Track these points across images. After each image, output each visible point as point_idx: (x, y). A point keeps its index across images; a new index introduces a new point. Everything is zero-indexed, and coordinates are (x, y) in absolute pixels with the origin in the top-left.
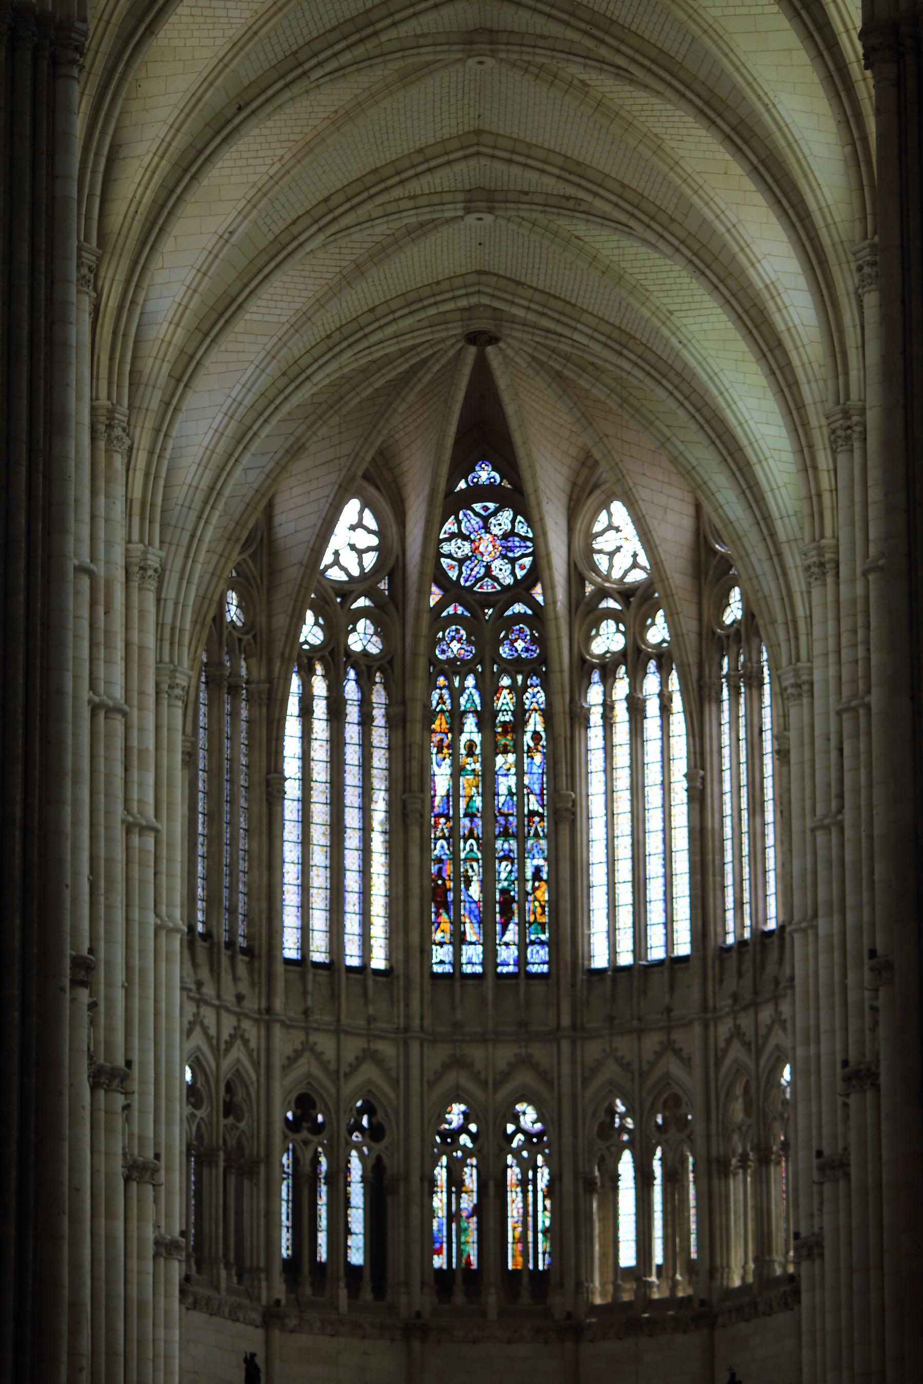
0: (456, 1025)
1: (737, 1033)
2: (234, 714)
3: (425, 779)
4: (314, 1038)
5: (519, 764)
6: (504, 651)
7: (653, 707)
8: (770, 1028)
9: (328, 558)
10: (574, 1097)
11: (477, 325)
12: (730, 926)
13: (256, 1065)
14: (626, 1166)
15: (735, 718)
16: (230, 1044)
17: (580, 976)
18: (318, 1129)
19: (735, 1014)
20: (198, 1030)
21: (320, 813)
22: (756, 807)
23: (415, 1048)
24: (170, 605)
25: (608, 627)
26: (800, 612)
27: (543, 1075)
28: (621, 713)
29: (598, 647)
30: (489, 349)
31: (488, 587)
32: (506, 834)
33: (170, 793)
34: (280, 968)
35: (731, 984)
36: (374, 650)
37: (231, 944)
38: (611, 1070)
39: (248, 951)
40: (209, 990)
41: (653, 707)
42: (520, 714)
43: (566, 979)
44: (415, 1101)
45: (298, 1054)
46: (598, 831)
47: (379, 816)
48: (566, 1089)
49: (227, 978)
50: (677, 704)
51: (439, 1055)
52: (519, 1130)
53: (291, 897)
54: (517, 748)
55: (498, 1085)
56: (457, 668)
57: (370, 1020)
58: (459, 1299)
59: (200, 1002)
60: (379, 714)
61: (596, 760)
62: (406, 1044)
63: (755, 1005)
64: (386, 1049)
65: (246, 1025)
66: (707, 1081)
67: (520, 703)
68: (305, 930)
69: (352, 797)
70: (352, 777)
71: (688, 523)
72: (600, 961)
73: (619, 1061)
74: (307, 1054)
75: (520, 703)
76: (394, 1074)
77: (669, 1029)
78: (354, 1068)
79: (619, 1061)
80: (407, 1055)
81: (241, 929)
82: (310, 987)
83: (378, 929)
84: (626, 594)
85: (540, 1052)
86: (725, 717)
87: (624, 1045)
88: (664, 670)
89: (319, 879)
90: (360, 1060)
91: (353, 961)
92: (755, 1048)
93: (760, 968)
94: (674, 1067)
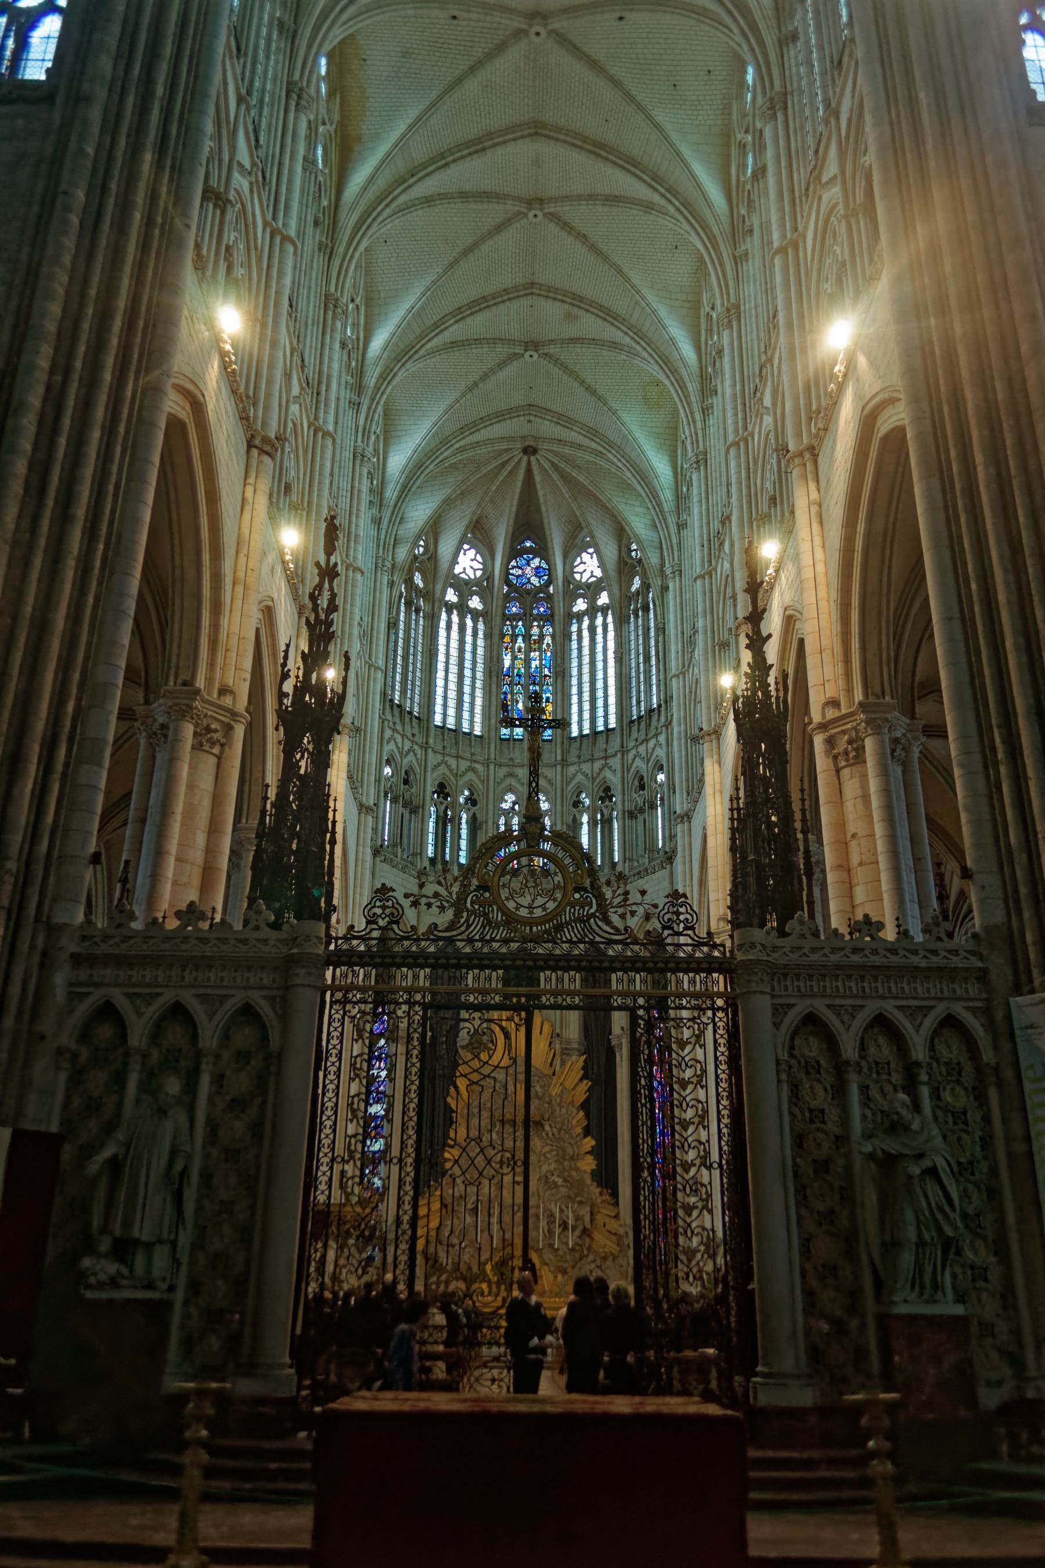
0: (511, 759)
2: (417, 621)
3: (500, 661)
4: (447, 758)
5: (540, 656)
6: (535, 612)
7: (600, 630)
11: (527, 444)
12: (635, 712)
13: (420, 766)
14: (585, 819)
15: (637, 627)
16: (408, 753)
19: (637, 746)
21: (454, 669)
22: (647, 659)
23: (492, 767)
24: (384, 532)
25: (580, 601)
26: (674, 541)
28: (586, 634)
29: (575, 609)
30: (533, 458)
31: (529, 586)
32: (534, 684)
33: (358, 504)
34: (432, 729)
35: (635, 735)
36: (480, 607)
37: (410, 713)
38: (580, 777)
40: (399, 727)
41: (600, 630)
42: (542, 637)
44: (491, 789)
45: (439, 764)
46: (574, 681)
47: (479, 675)
48: (559, 786)
49: (408, 727)
50: (611, 627)
51: (503, 771)
53: (439, 700)
54: (540, 650)
56: (515, 617)
57: (473, 754)
59: (394, 730)
60: (481, 634)
63: (647, 740)
64: (480, 767)
65: (416, 747)
67: (541, 632)
68: (445, 715)
69: (468, 664)
70: (468, 656)
71: (616, 552)
73: (583, 774)
74: (443, 766)
75: (541, 632)
77: (606, 758)
78: (464, 773)
79: (583, 774)
81: (416, 709)
83: (478, 718)
84: (588, 586)
86: (632, 628)
87: (586, 767)
88: (605, 616)
89: (452, 694)
90: (467, 771)
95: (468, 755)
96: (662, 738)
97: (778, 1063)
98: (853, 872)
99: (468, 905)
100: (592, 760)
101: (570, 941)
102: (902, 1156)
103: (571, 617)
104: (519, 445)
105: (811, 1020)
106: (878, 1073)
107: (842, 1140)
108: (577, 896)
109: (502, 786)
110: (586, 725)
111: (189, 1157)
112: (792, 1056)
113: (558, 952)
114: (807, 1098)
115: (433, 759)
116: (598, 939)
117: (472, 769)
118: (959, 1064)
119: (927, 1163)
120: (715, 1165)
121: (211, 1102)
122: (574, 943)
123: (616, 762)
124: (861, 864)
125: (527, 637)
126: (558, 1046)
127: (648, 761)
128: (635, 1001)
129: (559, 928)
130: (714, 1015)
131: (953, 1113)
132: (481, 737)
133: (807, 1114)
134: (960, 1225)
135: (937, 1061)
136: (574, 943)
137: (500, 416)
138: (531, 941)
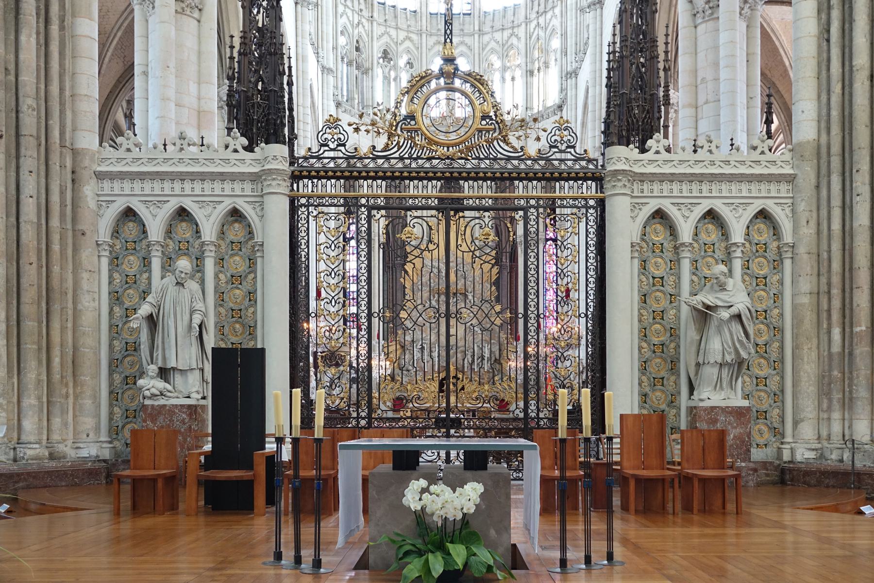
4: (388, 30)
8: (550, 20)
10: (479, 54)
17: (481, 13)
20: (345, 16)
23: (424, 36)
27: (469, 47)
38: (493, 44)
43: (477, 14)
45: (383, 34)
48: (477, 51)
57: (409, 26)
59: (346, 6)
62: (421, 35)
63: (545, 12)
64: (414, 37)
65: (364, 20)
66: (526, 44)
76: (417, 46)
77: (513, 28)
78: (403, 42)
80: (421, 40)
82: (387, 12)
85: (468, 40)
87: (498, 36)
90: (405, 40)
94: (514, 40)
95: (405, 27)
96: (557, 10)
97: (632, 246)
98: (699, 109)
99: (399, 132)
101: (478, 158)
102: (717, 306)
105: (659, 215)
106: (705, 251)
107: (673, 297)
108: (484, 122)
109: (433, 52)
111: (205, 315)
112: (643, 240)
113: (469, 166)
114: (652, 269)
115: (378, 30)
116: (499, 156)
117: (409, 38)
118: (765, 244)
119: (734, 310)
120: (583, 315)
121: (216, 276)
122: (482, 159)
123: (521, 32)
124: (707, 102)
127: (546, 29)
128: (528, 202)
129: (469, 149)
130: (587, 211)
131: (757, 278)
132: (415, 12)
133: (651, 280)
134: (753, 351)
135: (750, 243)
136: (482, 159)
138: (448, 158)
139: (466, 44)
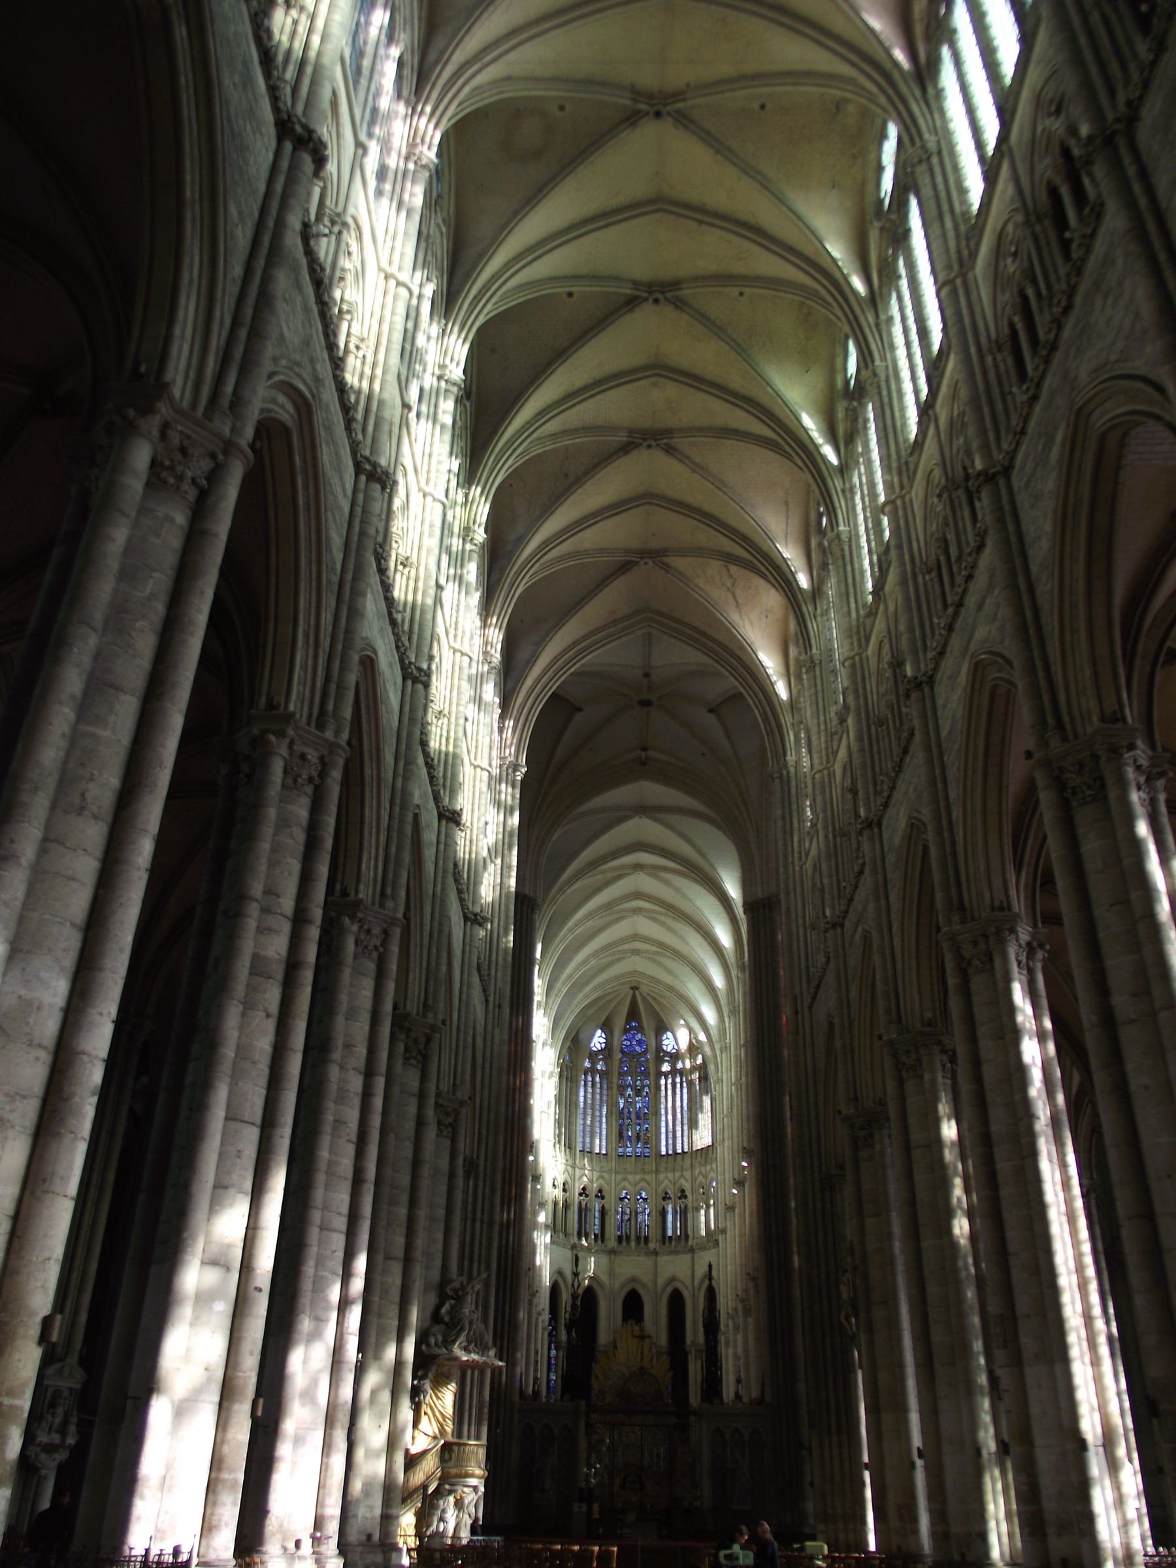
1: (700, 1173)
7: (678, 1085)
9: (592, 1045)
18: (587, 1196)
28: (669, 1087)
35: (699, 1158)
38: (667, 1182)
39: (570, 1148)
41: (678, 1085)
42: (643, 1086)
51: (620, 1177)
52: (641, 1198)
55: (635, 1186)
58: (624, 1243)
61: (663, 1100)
63: (705, 1165)
64: (605, 1175)
72: (664, 1153)
85: (647, 1177)
87: (670, 1175)
91: (597, 1151)
92: (705, 1177)
93: (707, 1154)
94: (683, 1181)
96: (714, 1166)
100: (674, 1170)
103: (660, 1074)
104: (629, 986)
110: (671, 1147)
123: (687, 1174)
125: (634, 1087)
126: (654, 1350)
137: (617, 978)
139: (646, 1181)
